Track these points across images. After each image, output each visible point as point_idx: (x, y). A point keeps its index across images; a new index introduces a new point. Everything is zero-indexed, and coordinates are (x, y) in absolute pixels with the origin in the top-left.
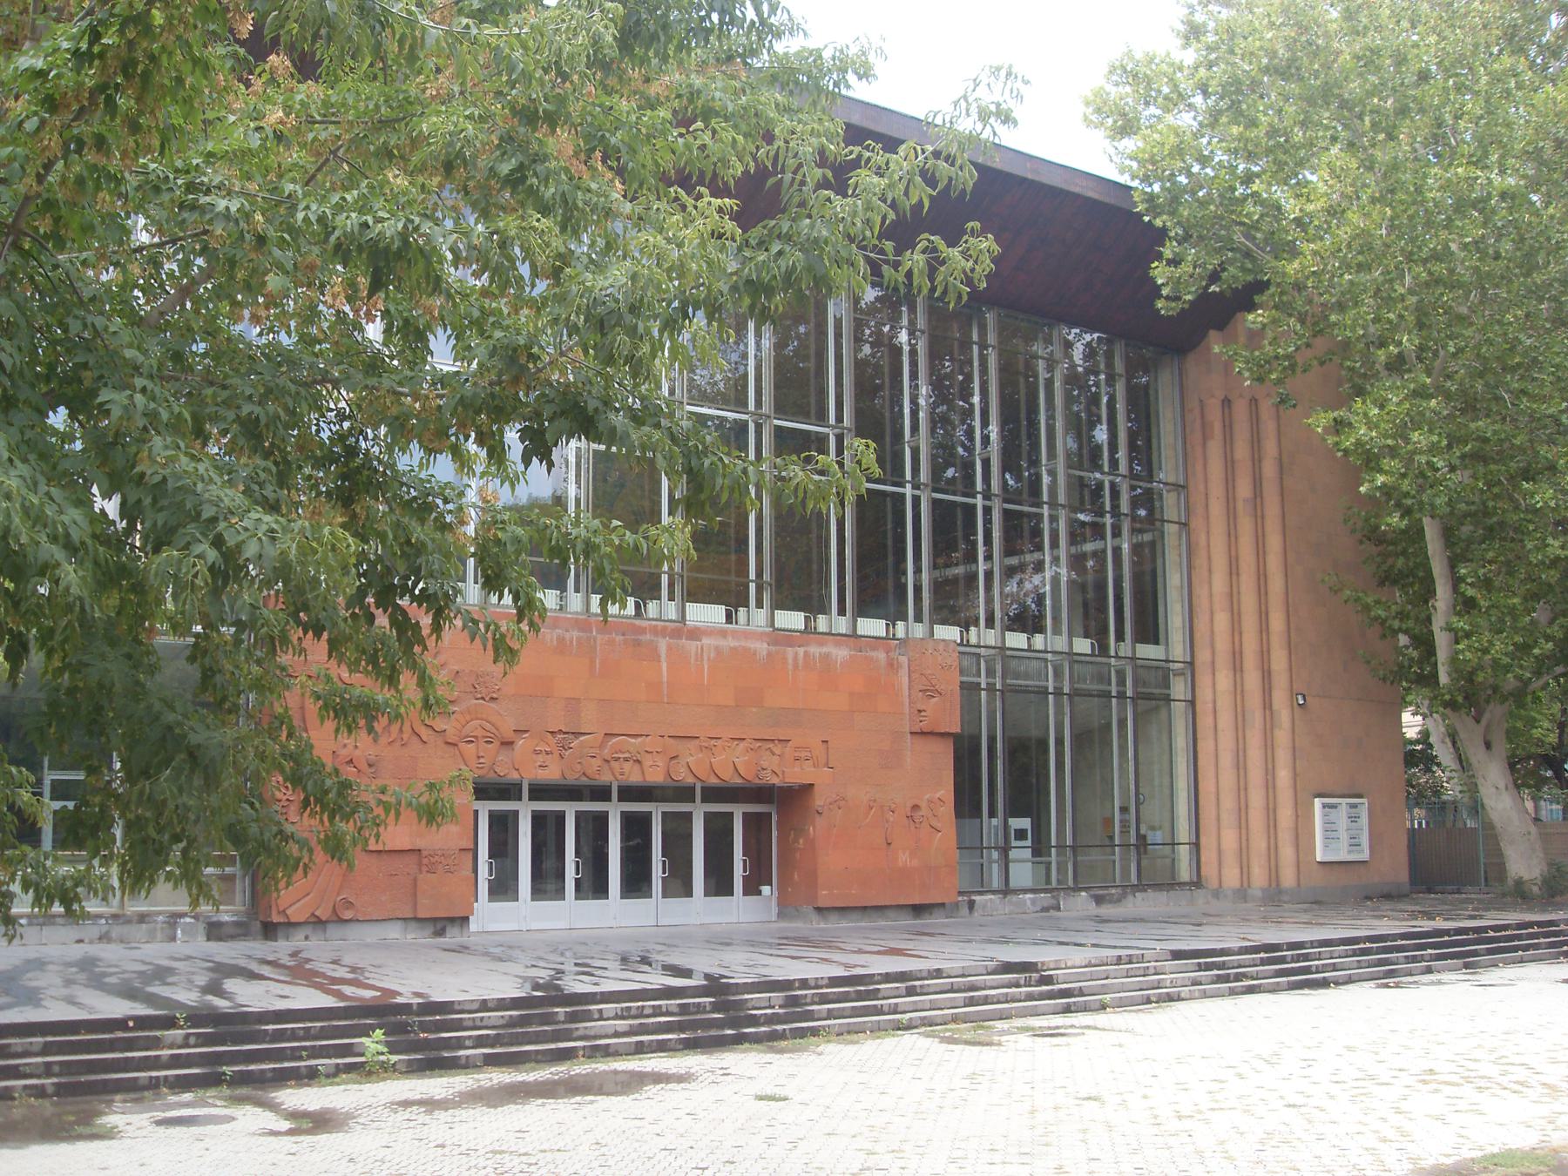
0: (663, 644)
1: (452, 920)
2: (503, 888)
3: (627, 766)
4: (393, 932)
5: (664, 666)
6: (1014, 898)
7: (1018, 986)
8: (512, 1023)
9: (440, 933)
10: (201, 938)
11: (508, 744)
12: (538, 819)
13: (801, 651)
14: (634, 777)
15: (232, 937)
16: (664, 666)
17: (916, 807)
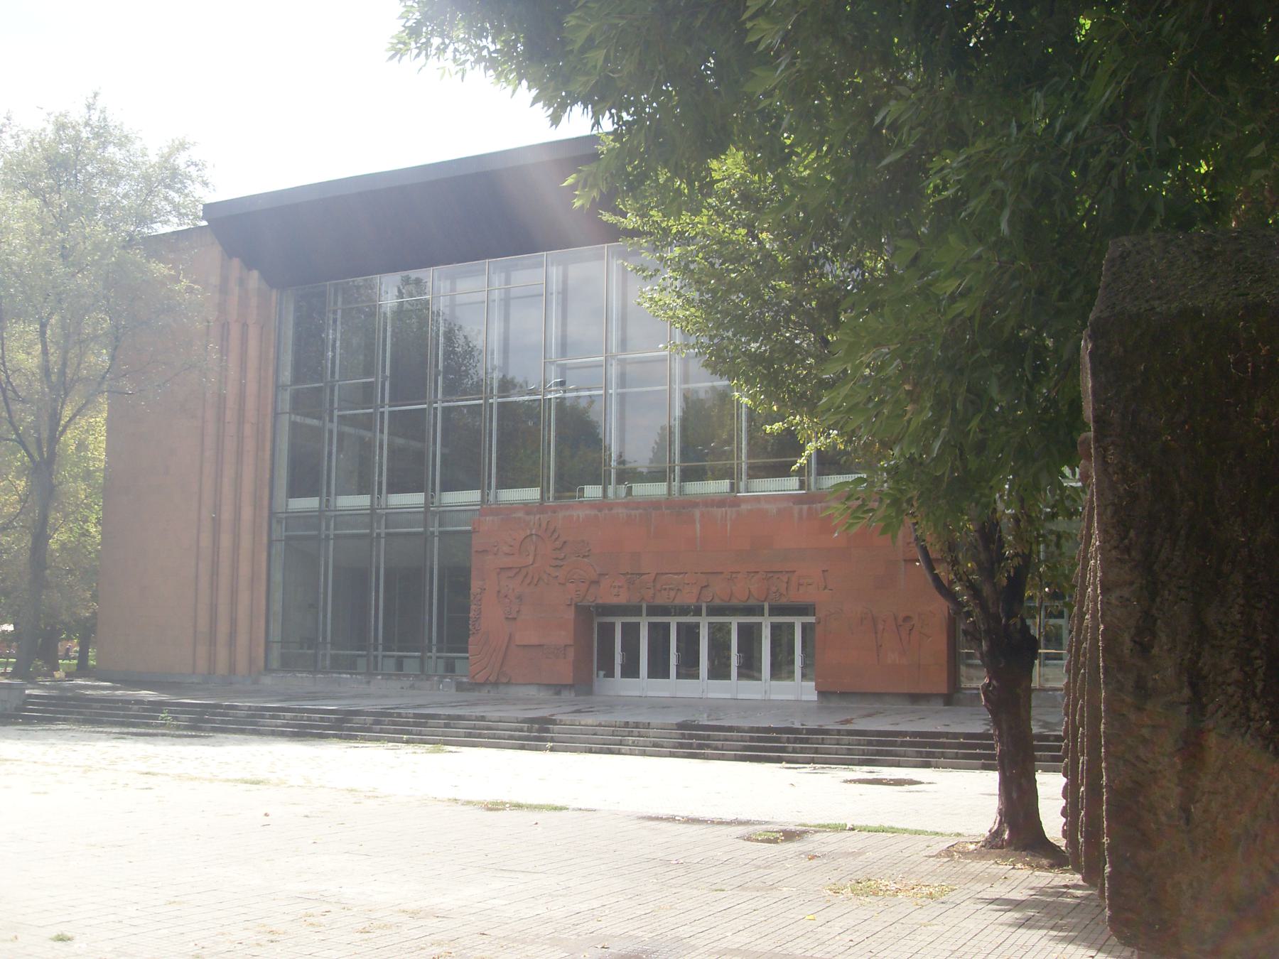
0: (697, 513)
1: (565, 686)
2: (631, 670)
3: (672, 594)
4: (532, 691)
5: (698, 526)
6: (1042, 694)
7: (522, 730)
8: (248, 716)
9: (558, 693)
10: (453, 690)
11: (596, 582)
12: (653, 627)
13: (805, 507)
14: (661, 600)
15: (469, 690)
16: (698, 526)
17: (907, 619)
